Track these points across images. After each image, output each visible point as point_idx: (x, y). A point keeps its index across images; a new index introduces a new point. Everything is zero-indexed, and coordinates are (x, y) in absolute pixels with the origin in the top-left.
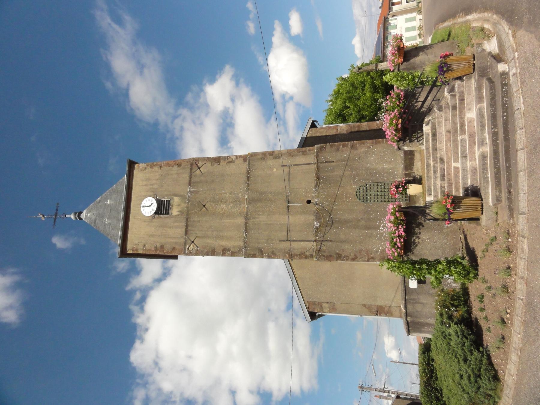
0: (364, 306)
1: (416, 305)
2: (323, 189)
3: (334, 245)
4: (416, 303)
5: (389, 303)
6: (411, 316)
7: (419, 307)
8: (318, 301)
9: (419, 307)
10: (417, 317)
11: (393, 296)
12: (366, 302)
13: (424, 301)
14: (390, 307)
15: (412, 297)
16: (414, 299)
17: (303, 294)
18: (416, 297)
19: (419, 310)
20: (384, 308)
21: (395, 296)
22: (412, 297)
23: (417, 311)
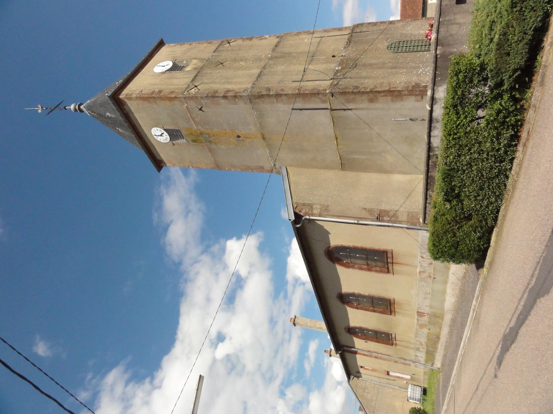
0: (365, 209)
1: (451, 27)
2: (352, 47)
3: (353, 81)
4: (451, 24)
5: (397, 208)
6: (443, 45)
7: (454, 29)
8: (310, 202)
9: (454, 29)
10: (449, 45)
11: (403, 202)
12: (368, 206)
13: (461, 21)
14: (396, 211)
15: (447, 18)
16: (449, 20)
17: (293, 196)
18: (452, 18)
19: (453, 32)
20: (389, 212)
21: (404, 202)
22: (447, 18)
23: (451, 35)
